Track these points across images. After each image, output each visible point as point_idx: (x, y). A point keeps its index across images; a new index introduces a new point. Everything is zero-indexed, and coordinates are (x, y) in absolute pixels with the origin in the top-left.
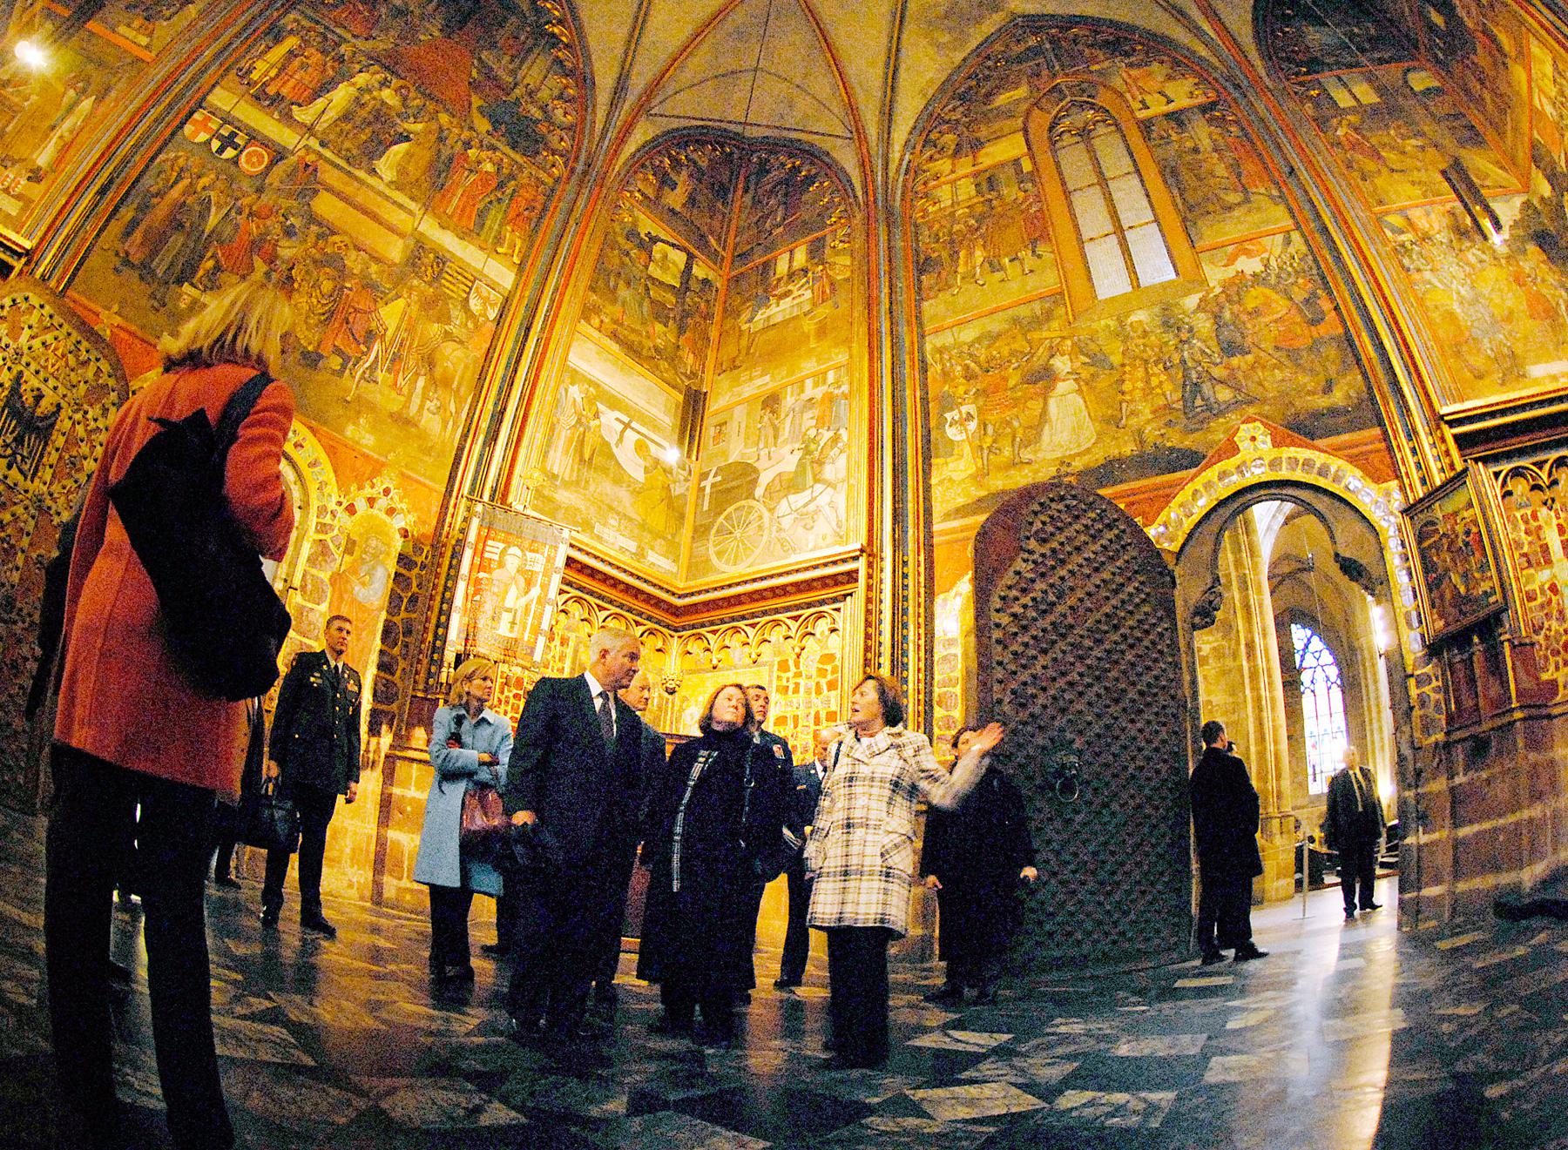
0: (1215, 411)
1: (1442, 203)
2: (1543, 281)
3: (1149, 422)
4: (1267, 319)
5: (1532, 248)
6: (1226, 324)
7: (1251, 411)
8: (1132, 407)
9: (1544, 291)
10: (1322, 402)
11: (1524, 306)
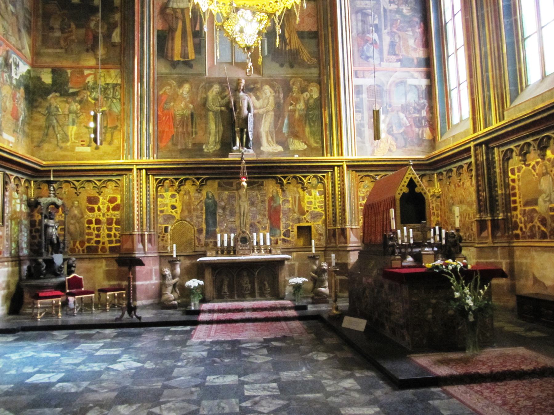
1: (7, 45)
2: (20, 104)
5: (22, 89)
9: (19, 108)
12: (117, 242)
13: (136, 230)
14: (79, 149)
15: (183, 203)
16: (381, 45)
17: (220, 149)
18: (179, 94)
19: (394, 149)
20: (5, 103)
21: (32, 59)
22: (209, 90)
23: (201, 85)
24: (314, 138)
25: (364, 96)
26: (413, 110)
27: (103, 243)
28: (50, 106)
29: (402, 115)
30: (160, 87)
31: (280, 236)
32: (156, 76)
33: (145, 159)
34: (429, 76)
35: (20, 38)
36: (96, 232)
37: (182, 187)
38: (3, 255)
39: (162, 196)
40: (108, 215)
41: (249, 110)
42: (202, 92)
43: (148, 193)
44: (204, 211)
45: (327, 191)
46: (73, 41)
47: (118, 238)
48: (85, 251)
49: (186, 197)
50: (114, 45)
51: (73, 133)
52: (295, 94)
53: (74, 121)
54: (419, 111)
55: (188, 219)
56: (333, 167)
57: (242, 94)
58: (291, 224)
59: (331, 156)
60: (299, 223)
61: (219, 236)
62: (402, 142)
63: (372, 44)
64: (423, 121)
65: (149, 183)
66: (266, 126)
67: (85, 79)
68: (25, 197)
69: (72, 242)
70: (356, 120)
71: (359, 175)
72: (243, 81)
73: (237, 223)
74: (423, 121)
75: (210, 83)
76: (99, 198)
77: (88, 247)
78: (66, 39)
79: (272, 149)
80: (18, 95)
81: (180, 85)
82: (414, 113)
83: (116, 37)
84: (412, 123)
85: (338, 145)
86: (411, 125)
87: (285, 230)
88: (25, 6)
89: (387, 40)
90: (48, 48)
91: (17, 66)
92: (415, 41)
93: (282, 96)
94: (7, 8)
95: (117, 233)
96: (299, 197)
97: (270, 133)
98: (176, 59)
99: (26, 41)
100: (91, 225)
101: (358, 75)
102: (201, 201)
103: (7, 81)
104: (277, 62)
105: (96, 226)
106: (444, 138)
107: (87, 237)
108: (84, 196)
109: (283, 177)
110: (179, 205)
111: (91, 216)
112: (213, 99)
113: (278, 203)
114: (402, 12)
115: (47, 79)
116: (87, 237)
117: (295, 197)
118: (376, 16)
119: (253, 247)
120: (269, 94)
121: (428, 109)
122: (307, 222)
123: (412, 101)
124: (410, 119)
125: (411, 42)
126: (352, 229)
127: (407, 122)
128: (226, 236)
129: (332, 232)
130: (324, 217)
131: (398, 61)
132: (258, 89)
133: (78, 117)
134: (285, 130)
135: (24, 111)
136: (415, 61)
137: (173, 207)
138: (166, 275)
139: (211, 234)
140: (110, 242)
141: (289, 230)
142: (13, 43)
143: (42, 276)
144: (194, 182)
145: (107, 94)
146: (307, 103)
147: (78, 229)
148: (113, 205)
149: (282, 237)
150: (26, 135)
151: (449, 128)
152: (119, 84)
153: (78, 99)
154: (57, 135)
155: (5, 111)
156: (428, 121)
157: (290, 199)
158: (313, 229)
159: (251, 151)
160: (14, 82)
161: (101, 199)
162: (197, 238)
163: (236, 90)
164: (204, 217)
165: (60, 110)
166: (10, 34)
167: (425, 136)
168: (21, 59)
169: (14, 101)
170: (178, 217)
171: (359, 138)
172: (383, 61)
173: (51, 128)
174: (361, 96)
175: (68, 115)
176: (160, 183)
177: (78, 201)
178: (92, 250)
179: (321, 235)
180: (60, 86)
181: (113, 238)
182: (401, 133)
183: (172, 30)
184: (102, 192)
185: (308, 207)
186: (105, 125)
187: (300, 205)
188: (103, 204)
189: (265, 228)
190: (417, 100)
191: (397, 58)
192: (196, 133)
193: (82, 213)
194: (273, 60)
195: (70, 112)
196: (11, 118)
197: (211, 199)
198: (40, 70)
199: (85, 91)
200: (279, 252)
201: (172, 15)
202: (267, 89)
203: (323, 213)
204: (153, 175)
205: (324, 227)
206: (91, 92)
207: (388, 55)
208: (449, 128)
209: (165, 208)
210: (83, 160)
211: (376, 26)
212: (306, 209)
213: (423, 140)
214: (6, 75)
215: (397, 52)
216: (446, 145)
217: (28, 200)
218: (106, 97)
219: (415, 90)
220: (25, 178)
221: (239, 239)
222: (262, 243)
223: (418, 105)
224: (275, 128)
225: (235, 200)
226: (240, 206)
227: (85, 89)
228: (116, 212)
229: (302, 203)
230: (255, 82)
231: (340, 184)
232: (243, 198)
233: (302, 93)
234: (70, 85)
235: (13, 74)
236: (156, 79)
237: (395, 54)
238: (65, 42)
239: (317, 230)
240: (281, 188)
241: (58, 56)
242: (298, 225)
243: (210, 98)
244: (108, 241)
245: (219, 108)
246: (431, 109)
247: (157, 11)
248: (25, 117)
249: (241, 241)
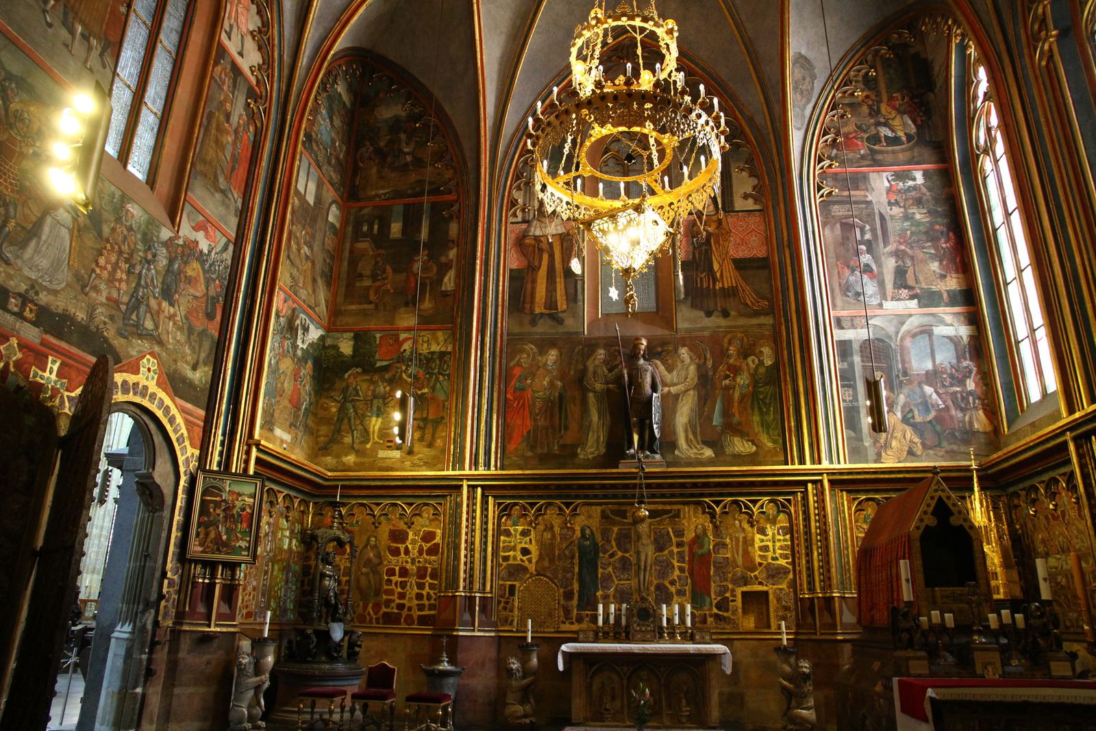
0: (138, 332)
1: (294, 301)
3: (102, 304)
4: (192, 291)
5: (310, 364)
6: (173, 272)
7: (157, 349)
8: (97, 282)
10: (190, 374)
11: (290, 393)
12: (431, 607)
13: (461, 589)
14: (382, 454)
15: (541, 544)
16: (881, 273)
17: (605, 454)
18: (541, 365)
19: (918, 450)
20: (282, 384)
21: (330, 319)
22: (588, 359)
23: (576, 350)
24: (768, 433)
25: (857, 359)
26: (948, 379)
27: (410, 609)
28: (348, 387)
29: (928, 390)
30: (511, 356)
31: (710, 609)
32: (505, 338)
33: (482, 471)
34: (974, 319)
35: (314, 291)
36: (399, 590)
37: (540, 518)
38: (255, 619)
39: (508, 533)
40: (419, 562)
41: (654, 388)
42: (577, 361)
43: (484, 526)
44: (576, 561)
45: (795, 528)
46: (388, 291)
47: (432, 602)
48: (381, 621)
49: (548, 535)
50: (445, 294)
51: (377, 428)
52: (731, 361)
53: (379, 409)
54: (961, 382)
55: (548, 574)
56: (804, 483)
57: (642, 361)
58: (730, 586)
59: (800, 463)
60: (745, 585)
61: (601, 607)
62: (931, 438)
63: (865, 272)
64: (971, 399)
65: (487, 509)
66: (683, 416)
67: (401, 346)
68: (298, 527)
69: (361, 603)
70: (844, 401)
71: (854, 499)
72: (644, 342)
73: (634, 583)
74: (971, 399)
75: (590, 346)
76: (408, 534)
77: (385, 613)
78: (377, 291)
79: (695, 454)
80: (303, 372)
81: (542, 351)
82: (952, 385)
83: (449, 282)
84: (950, 403)
85: (811, 445)
86: (947, 408)
87: (719, 598)
88: (327, 247)
89: (890, 264)
90: (352, 303)
91: (306, 330)
92: (941, 263)
93: (710, 364)
94: (299, 251)
95: (431, 592)
96: (745, 538)
97: (691, 426)
98: (537, 311)
99: (322, 295)
100: (392, 578)
101: (844, 324)
102: (572, 542)
103: (288, 352)
104: (701, 308)
105: (400, 579)
106: (1015, 428)
107: (385, 597)
108: (384, 530)
109: (714, 502)
110: (533, 548)
111: (394, 562)
113: (706, 547)
114: (912, 218)
115: (346, 348)
116: (385, 597)
117: (737, 540)
118: (868, 227)
119: (661, 628)
120: (688, 360)
121: (979, 376)
122: (760, 583)
123: (946, 364)
124: (944, 396)
125: (935, 266)
126: (844, 598)
127: (940, 403)
128: (612, 608)
129: (807, 604)
130: (791, 576)
131: (912, 297)
132: (668, 352)
133: (385, 404)
134: (717, 420)
135: (310, 395)
136: (945, 295)
137: (525, 552)
138: (512, 669)
139: (588, 603)
140: (421, 607)
141: (727, 598)
142: (304, 297)
143: (309, 659)
144: (560, 509)
145: (431, 368)
146: (753, 376)
147: (373, 583)
148: (429, 545)
149: (715, 610)
150: (309, 431)
151: (1022, 410)
152: (450, 353)
153: (387, 376)
154: (353, 431)
155: (281, 396)
156: (979, 398)
157: (728, 541)
158: (771, 597)
159: (658, 457)
160: (299, 353)
161: (411, 536)
162: (563, 607)
163: (633, 356)
164: (577, 570)
166: (301, 285)
167: (976, 426)
168: (312, 320)
169: (296, 380)
170: (532, 568)
171: (852, 434)
172: (886, 300)
173: (346, 421)
174: (849, 359)
175: (372, 401)
176: (505, 511)
177: (376, 537)
178: (390, 619)
179: (786, 608)
180: (363, 360)
181: (426, 602)
182: (930, 422)
183: (533, 269)
184: (413, 523)
185: (760, 556)
186: (425, 416)
187: (746, 553)
188: (414, 542)
189: (680, 593)
190: (954, 361)
191: (911, 293)
192: (566, 428)
193: (379, 556)
194: (694, 306)
195: (375, 397)
196: (290, 406)
197: (587, 539)
198: (337, 335)
199: (398, 365)
200: (708, 638)
201: (534, 246)
202: (684, 352)
203: (790, 567)
204: (495, 497)
205: (792, 594)
206: (408, 366)
207: (894, 288)
208: (1022, 410)
209: (511, 553)
210: (387, 470)
211: (869, 244)
212: (758, 560)
213: (974, 433)
214: (287, 343)
215: (911, 282)
216: (1019, 440)
217: (303, 532)
218: (428, 373)
219: (951, 347)
220: (301, 497)
221: (635, 611)
222: (677, 621)
223: (957, 371)
224: (700, 417)
225: (630, 542)
226: (638, 553)
227: (398, 362)
228: (433, 558)
229: (750, 548)
230: (664, 343)
231: (818, 515)
232: (645, 540)
233: (746, 357)
234: (377, 357)
235: (299, 343)
236: (505, 343)
237: (906, 287)
238: (376, 294)
239: (779, 600)
240: (711, 522)
241: (365, 314)
242: (745, 589)
243: (591, 369)
244: (418, 605)
245: (603, 386)
246: (986, 378)
247: (510, 242)
248: (311, 404)
249: (639, 617)
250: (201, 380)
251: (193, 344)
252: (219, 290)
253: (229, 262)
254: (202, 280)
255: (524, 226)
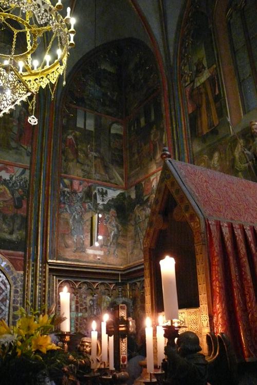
5: (113, 210)
10: (8, 237)
112: (240, 157)
165: (141, 218)
243: (237, 156)
250: (17, 238)
251: (8, 222)
252: (22, 193)
253: (28, 178)
254: (8, 191)
255: (192, 85)
